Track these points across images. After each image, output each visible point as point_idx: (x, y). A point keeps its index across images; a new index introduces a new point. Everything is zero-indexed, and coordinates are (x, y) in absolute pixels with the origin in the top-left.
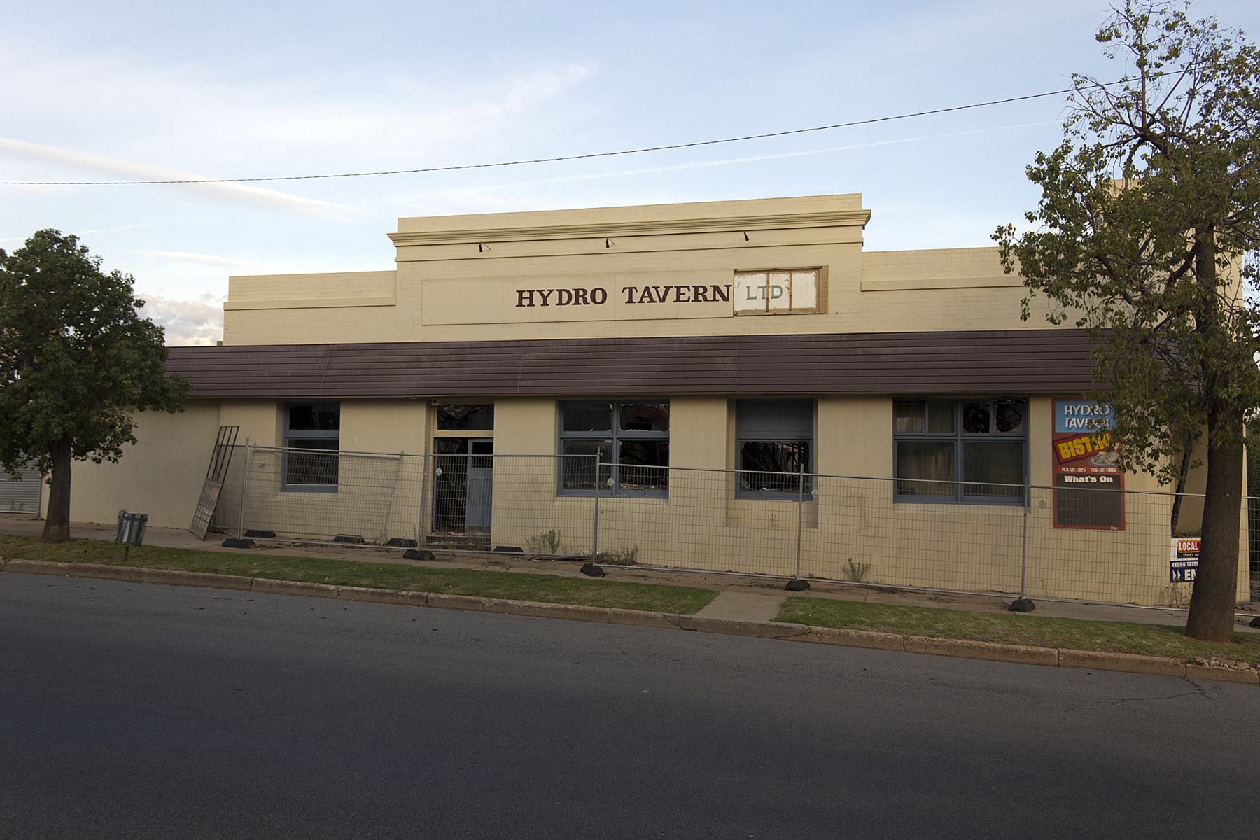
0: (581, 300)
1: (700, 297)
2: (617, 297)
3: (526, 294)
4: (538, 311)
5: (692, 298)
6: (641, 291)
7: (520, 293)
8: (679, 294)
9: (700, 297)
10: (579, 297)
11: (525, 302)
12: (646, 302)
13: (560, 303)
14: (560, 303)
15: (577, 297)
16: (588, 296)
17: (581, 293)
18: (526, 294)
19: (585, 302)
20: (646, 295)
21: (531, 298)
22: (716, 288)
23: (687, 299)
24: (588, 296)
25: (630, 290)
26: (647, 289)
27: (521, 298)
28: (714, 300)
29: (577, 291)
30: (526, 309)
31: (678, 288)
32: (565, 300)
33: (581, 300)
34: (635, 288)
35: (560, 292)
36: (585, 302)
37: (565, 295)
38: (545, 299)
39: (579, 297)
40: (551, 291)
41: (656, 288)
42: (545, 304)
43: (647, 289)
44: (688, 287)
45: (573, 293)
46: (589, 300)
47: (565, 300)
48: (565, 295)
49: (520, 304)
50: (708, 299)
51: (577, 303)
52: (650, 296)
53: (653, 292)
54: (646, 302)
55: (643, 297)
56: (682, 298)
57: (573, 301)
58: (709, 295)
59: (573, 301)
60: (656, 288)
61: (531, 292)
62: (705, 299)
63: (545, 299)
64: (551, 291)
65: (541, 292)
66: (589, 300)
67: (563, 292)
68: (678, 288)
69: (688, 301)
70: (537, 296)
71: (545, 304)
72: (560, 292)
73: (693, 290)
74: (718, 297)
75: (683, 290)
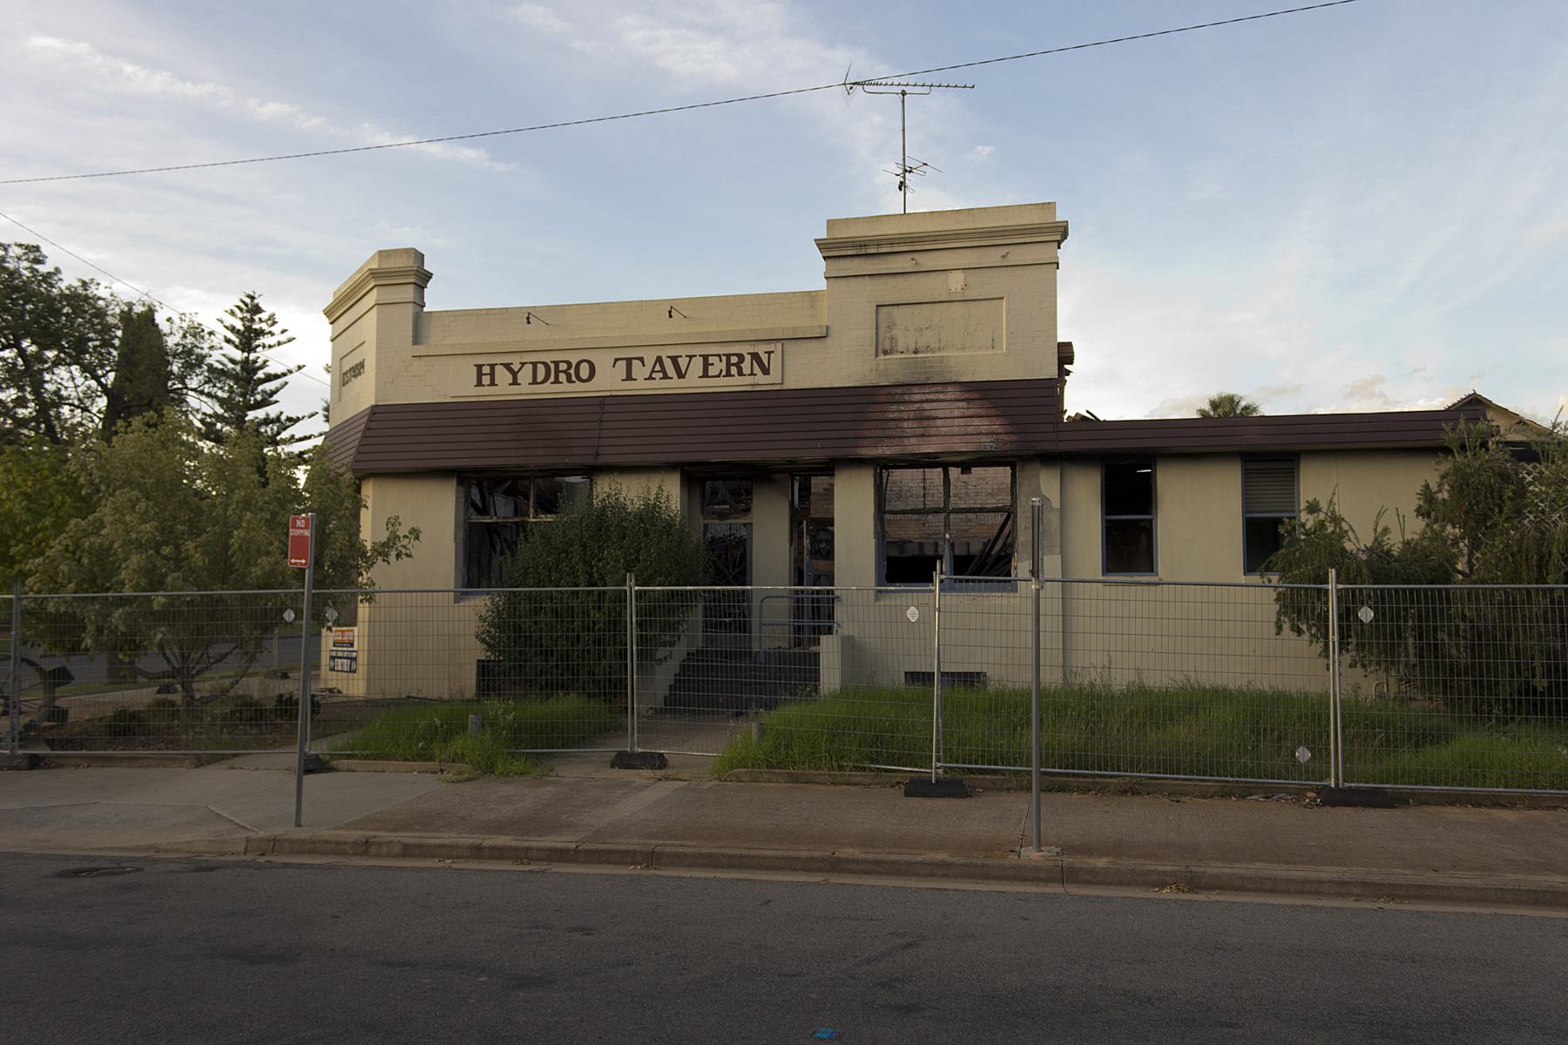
0: (562, 377)
1: (734, 370)
3: (486, 370)
5: (724, 373)
6: (650, 361)
7: (479, 367)
8: (706, 365)
9: (734, 370)
11: (486, 380)
14: (535, 382)
15: (557, 371)
18: (486, 370)
19: (569, 380)
20: (658, 368)
21: (492, 374)
22: (755, 356)
23: (717, 373)
26: (659, 360)
27: (480, 375)
28: (752, 374)
29: (557, 364)
31: (705, 358)
32: (541, 376)
33: (562, 377)
34: (641, 359)
35: (535, 365)
37: (541, 368)
38: (515, 374)
40: (523, 364)
43: (659, 360)
44: (719, 356)
45: (552, 366)
47: (541, 376)
48: (541, 368)
50: (744, 373)
52: (663, 370)
54: (657, 379)
55: (653, 371)
56: (712, 371)
57: (552, 379)
58: (746, 367)
59: (552, 379)
61: (492, 366)
62: (740, 373)
63: (515, 374)
64: (523, 364)
65: (508, 366)
66: (574, 378)
67: (539, 365)
68: (705, 358)
69: (719, 376)
70: (499, 370)
72: (535, 365)
73: (724, 358)
74: (757, 369)
75: (711, 360)
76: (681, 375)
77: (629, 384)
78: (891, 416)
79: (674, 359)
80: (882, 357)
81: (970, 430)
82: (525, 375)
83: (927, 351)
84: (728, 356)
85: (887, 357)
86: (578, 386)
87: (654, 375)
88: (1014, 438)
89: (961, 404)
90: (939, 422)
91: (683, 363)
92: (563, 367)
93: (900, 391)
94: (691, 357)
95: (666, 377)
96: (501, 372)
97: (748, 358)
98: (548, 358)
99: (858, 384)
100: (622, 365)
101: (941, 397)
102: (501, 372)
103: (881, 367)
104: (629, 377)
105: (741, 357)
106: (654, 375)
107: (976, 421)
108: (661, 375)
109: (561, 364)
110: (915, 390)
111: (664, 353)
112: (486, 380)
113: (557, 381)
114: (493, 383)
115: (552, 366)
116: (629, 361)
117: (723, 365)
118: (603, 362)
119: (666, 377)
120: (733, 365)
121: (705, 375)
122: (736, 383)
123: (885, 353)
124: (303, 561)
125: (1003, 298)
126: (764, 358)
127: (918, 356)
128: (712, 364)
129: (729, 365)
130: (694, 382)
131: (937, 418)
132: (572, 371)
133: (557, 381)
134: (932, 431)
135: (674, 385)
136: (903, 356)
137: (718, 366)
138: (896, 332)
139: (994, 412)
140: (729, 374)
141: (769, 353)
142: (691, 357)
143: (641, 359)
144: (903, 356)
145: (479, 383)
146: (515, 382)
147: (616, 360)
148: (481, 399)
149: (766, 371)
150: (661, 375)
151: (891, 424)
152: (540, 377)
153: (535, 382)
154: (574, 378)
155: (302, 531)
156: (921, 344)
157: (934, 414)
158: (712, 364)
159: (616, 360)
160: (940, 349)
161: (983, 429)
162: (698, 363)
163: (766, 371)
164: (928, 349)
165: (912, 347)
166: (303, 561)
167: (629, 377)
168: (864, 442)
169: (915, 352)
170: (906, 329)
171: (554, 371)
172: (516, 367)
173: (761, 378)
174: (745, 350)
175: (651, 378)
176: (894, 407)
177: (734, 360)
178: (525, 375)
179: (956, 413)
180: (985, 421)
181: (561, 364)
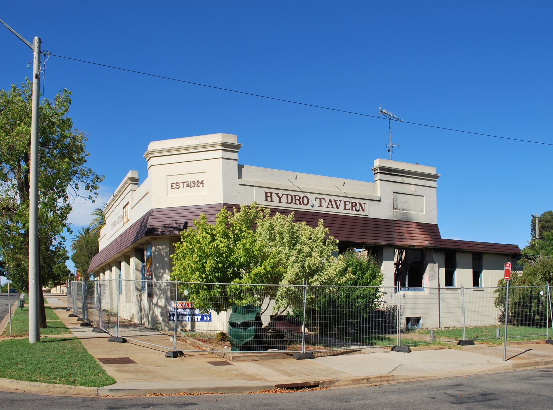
0: (297, 202)
1: (354, 208)
3: (269, 195)
5: (351, 209)
6: (327, 201)
7: (266, 193)
8: (345, 205)
11: (269, 199)
12: (330, 208)
14: (287, 203)
15: (296, 200)
18: (269, 195)
19: (300, 204)
20: (330, 204)
21: (271, 197)
22: (360, 204)
23: (349, 209)
26: (330, 200)
27: (267, 196)
29: (295, 196)
31: (345, 202)
33: (297, 202)
34: (324, 199)
35: (287, 195)
37: (290, 197)
38: (280, 198)
40: (283, 194)
43: (330, 200)
44: (349, 202)
47: (290, 201)
48: (290, 197)
52: (332, 205)
54: (330, 208)
55: (328, 205)
56: (348, 207)
57: (294, 202)
59: (294, 202)
61: (271, 193)
63: (280, 198)
64: (283, 194)
65: (277, 194)
66: (302, 203)
68: (345, 202)
69: (349, 210)
70: (274, 195)
72: (287, 195)
73: (351, 203)
75: (347, 203)
76: (338, 208)
77: (320, 209)
78: (401, 231)
79: (335, 201)
80: (394, 210)
81: (422, 238)
82: (284, 199)
83: (405, 210)
84: (352, 202)
85: (396, 210)
86: (303, 207)
87: (329, 206)
88: (433, 242)
89: (418, 230)
90: (414, 235)
91: (338, 202)
92: (298, 198)
93: (401, 222)
94: (341, 201)
95: (333, 207)
96: (275, 197)
97: (358, 204)
98: (293, 193)
99: (389, 219)
100: (318, 200)
101: (412, 226)
102: (275, 197)
103: (395, 214)
104: (321, 206)
105: (356, 203)
106: (329, 206)
107: (423, 236)
108: (331, 206)
109: (297, 197)
110: (405, 223)
111: (333, 198)
112: (269, 199)
113: (295, 203)
114: (272, 201)
115: (294, 197)
116: (321, 199)
117: (350, 206)
118: (312, 197)
119: (333, 207)
120: (354, 206)
121: (345, 209)
122: (354, 213)
123: (395, 209)
124: (508, 278)
125: (424, 196)
126: (363, 205)
127: (404, 211)
128: (347, 205)
129: (352, 206)
130: (341, 211)
131: (413, 234)
132: (301, 200)
133: (295, 203)
134: (413, 238)
135: (335, 211)
136: (400, 211)
137: (349, 206)
138: (398, 202)
139: (426, 233)
140: (352, 210)
141: (364, 204)
142: (341, 201)
143: (324, 199)
144: (400, 211)
145: (267, 200)
146: (280, 202)
147: (316, 198)
149: (363, 210)
150: (331, 206)
151: (401, 234)
152: (290, 201)
153: (287, 203)
154: (302, 203)
155: (508, 268)
156: (404, 208)
157: (412, 232)
158: (347, 205)
159: (316, 198)
160: (409, 210)
161: (425, 239)
162: (343, 204)
163: (363, 210)
164: (406, 210)
165: (402, 208)
166: (508, 278)
167: (321, 206)
168: (397, 240)
169: (403, 210)
170: (401, 202)
171: (294, 199)
172: (280, 195)
173: (361, 212)
174: (357, 201)
175: (328, 207)
176: (401, 228)
177: (354, 204)
178: (284, 199)
179: (417, 232)
180: (425, 236)
181: (297, 197)
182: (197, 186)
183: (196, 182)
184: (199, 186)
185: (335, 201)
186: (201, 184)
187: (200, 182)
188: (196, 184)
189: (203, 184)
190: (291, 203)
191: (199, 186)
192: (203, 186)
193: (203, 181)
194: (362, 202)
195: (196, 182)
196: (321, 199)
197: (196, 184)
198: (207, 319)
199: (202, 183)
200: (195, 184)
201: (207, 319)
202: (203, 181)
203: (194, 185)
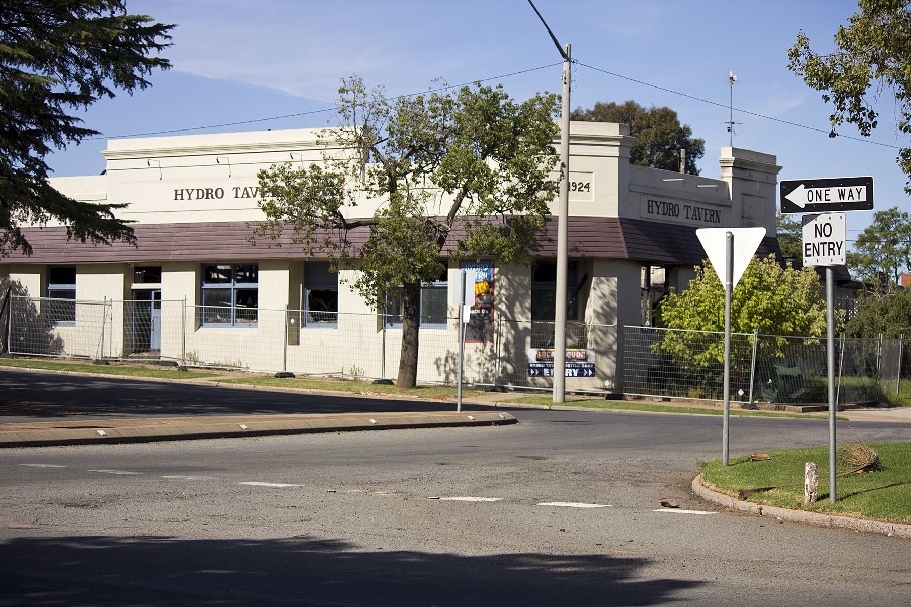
2: (229, 194)
4: (185, 204)
7: (649, 201)
10: (208, 194)
13: (198, 198)
16: (214, 193)
17: (210, 191)
24: (214, 193)
25: (237, 189)
29: (669, 204)
30: (179, 202)
34: (690, 207)
36: (212, 198)
39: (208, 194)
40: (661, 202)
41: (251, 188)
42: (190, 199)
46: (214, 196)
49: (176, 199)
51: (207, 198)
53: (697, 210)
60: (251, 188)
65: (656, 202)
71: (190, 199)
84: (711, 210)
98: (667, 201)
119: (696, 219)
126: (719, 213)
127: (750, 221)
133: (669, 215)
141: (720, 211)
142: (702, 209)
146: (658, 213)
148: (649, 220)
174: (714, 208)
182: (579, 190)
183: (578, 184)
184: (582, 191)
185: (698, 208)
186: (585, 187)
187: (584, 185)
188: (578, 187)
189: (588, 188)
190: (665, 215)
191: (582, 191)
192: (588, 191)
193: (588, 184)
194: (718, 209)
195: (578, 184)
196: (688, 207)
197: (578, 187)
198: (535, 373)
199: (587, 186)
200: (576, 186)
201: (535, 373)
202: (588, 184)
203: (574, 188)
